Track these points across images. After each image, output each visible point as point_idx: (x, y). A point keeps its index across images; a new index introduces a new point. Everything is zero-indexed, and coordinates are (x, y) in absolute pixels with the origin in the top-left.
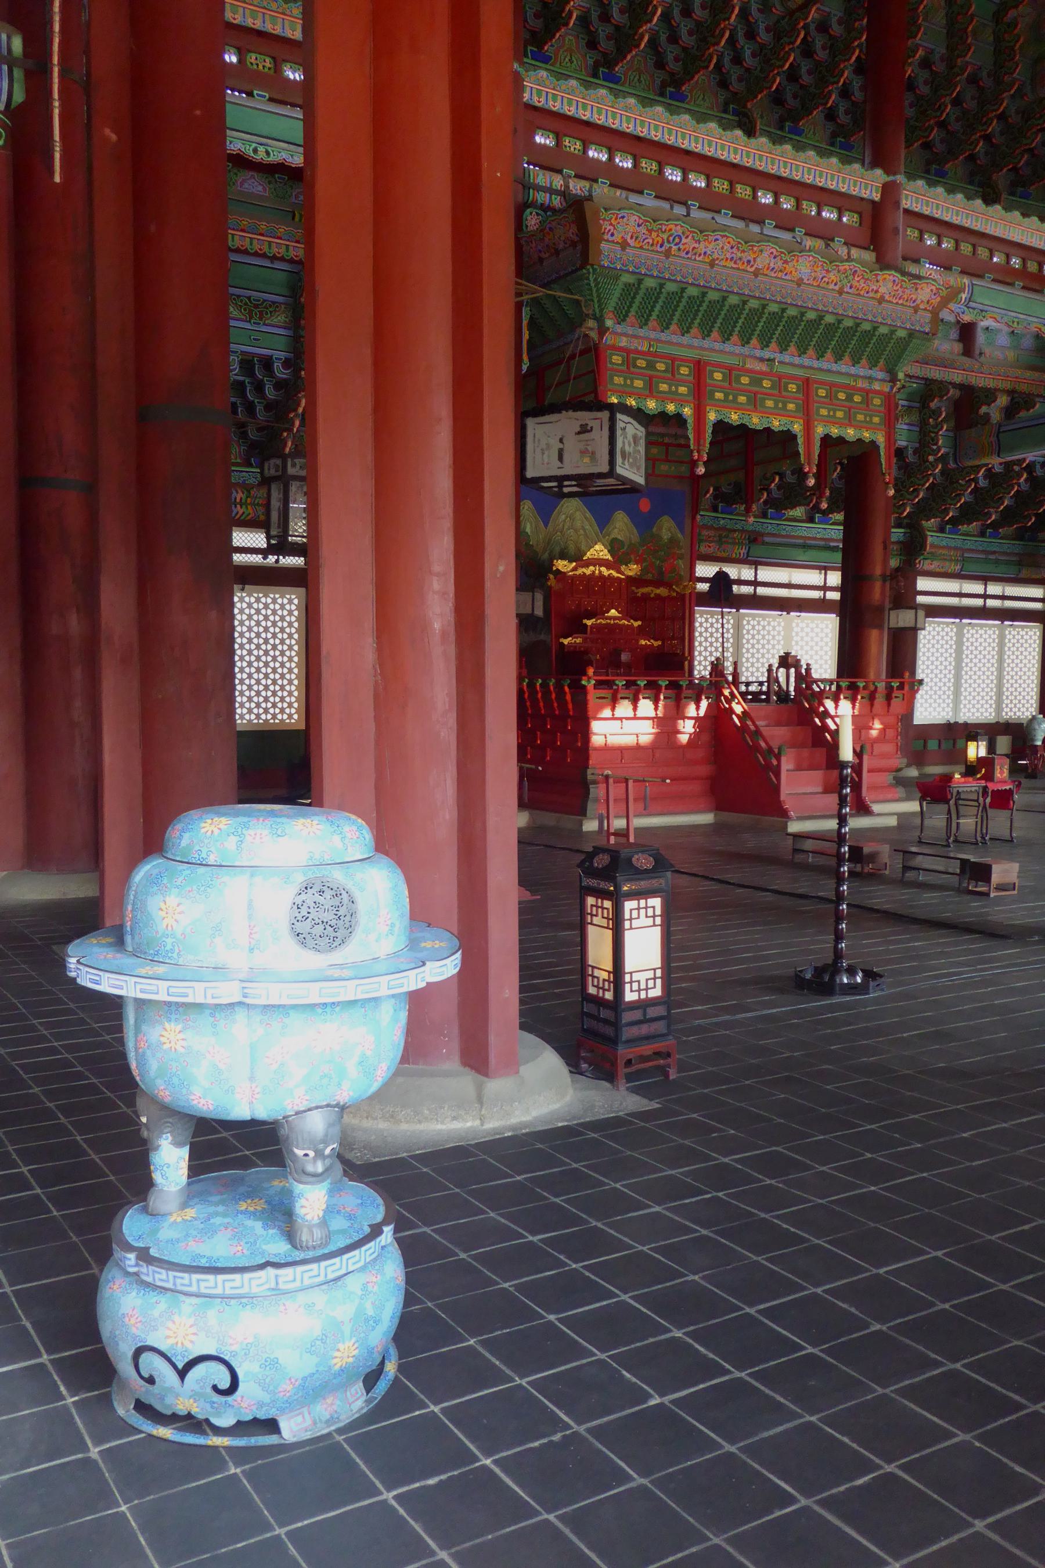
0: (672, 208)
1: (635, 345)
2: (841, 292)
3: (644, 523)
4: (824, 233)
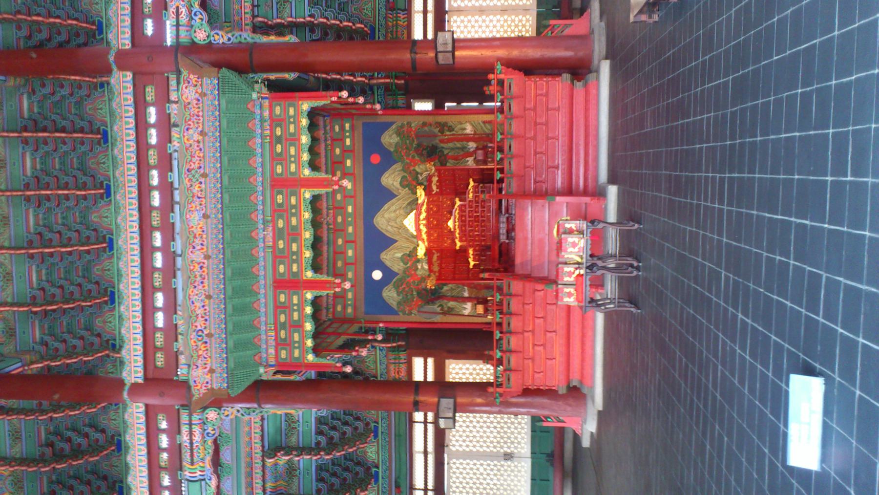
0: (177, 189)
1: (272, 342)
2: (204, 175)
3: (388, 159)
4: (166, 125)
